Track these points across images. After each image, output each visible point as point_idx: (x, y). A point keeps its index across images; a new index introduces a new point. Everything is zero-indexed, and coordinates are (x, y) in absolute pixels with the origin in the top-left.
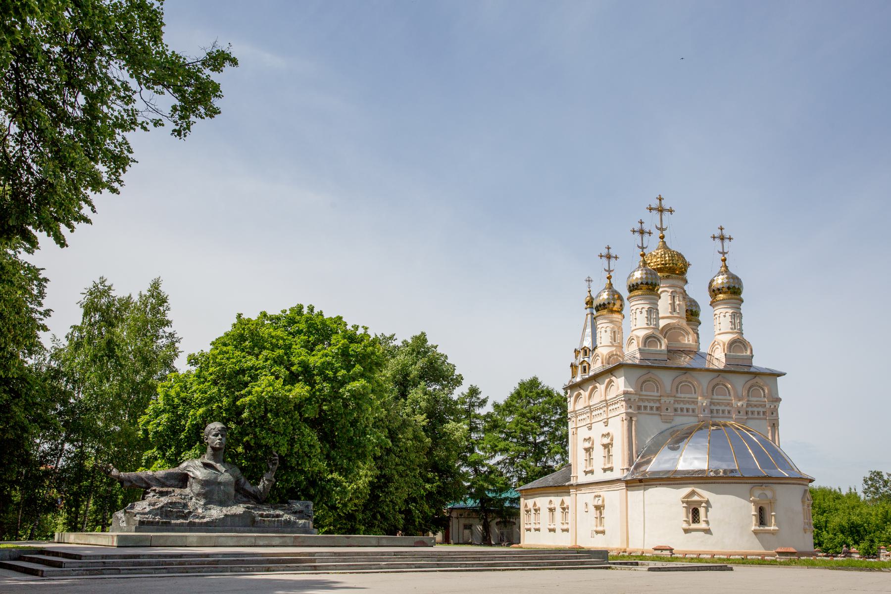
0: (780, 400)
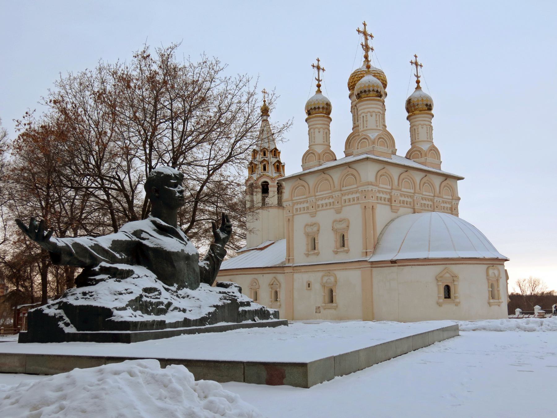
0: (459, 199)
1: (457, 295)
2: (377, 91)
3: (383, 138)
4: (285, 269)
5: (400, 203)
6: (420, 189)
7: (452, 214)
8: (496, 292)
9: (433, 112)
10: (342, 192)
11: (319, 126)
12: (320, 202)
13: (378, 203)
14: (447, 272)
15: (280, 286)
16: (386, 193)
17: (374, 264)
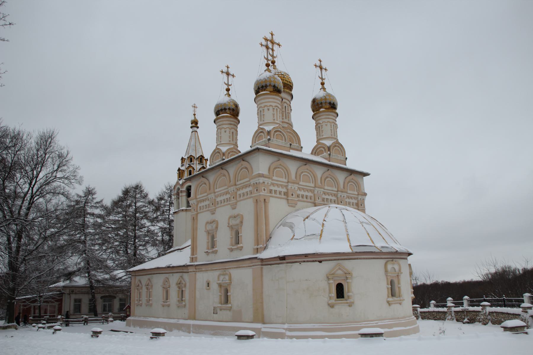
0: (365, 194)
1: (350, 294)
2: (274, 86)
3: (281, 132)
4: (189, 268)
5: (298, 196)
6: (321, 183)
7: (358, 210)
8: (397, 290)
9: (338, 111)
10: (237, 187)
11: (225, 126)
12: (219, 199)
13: (271, 196)
14: (340, 269)
15: (185, 286)
16: (282, 185)
17: (264, 262)
